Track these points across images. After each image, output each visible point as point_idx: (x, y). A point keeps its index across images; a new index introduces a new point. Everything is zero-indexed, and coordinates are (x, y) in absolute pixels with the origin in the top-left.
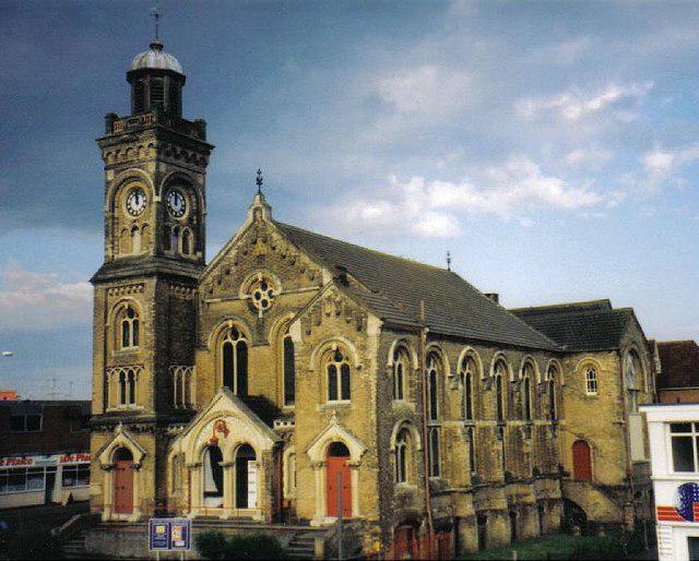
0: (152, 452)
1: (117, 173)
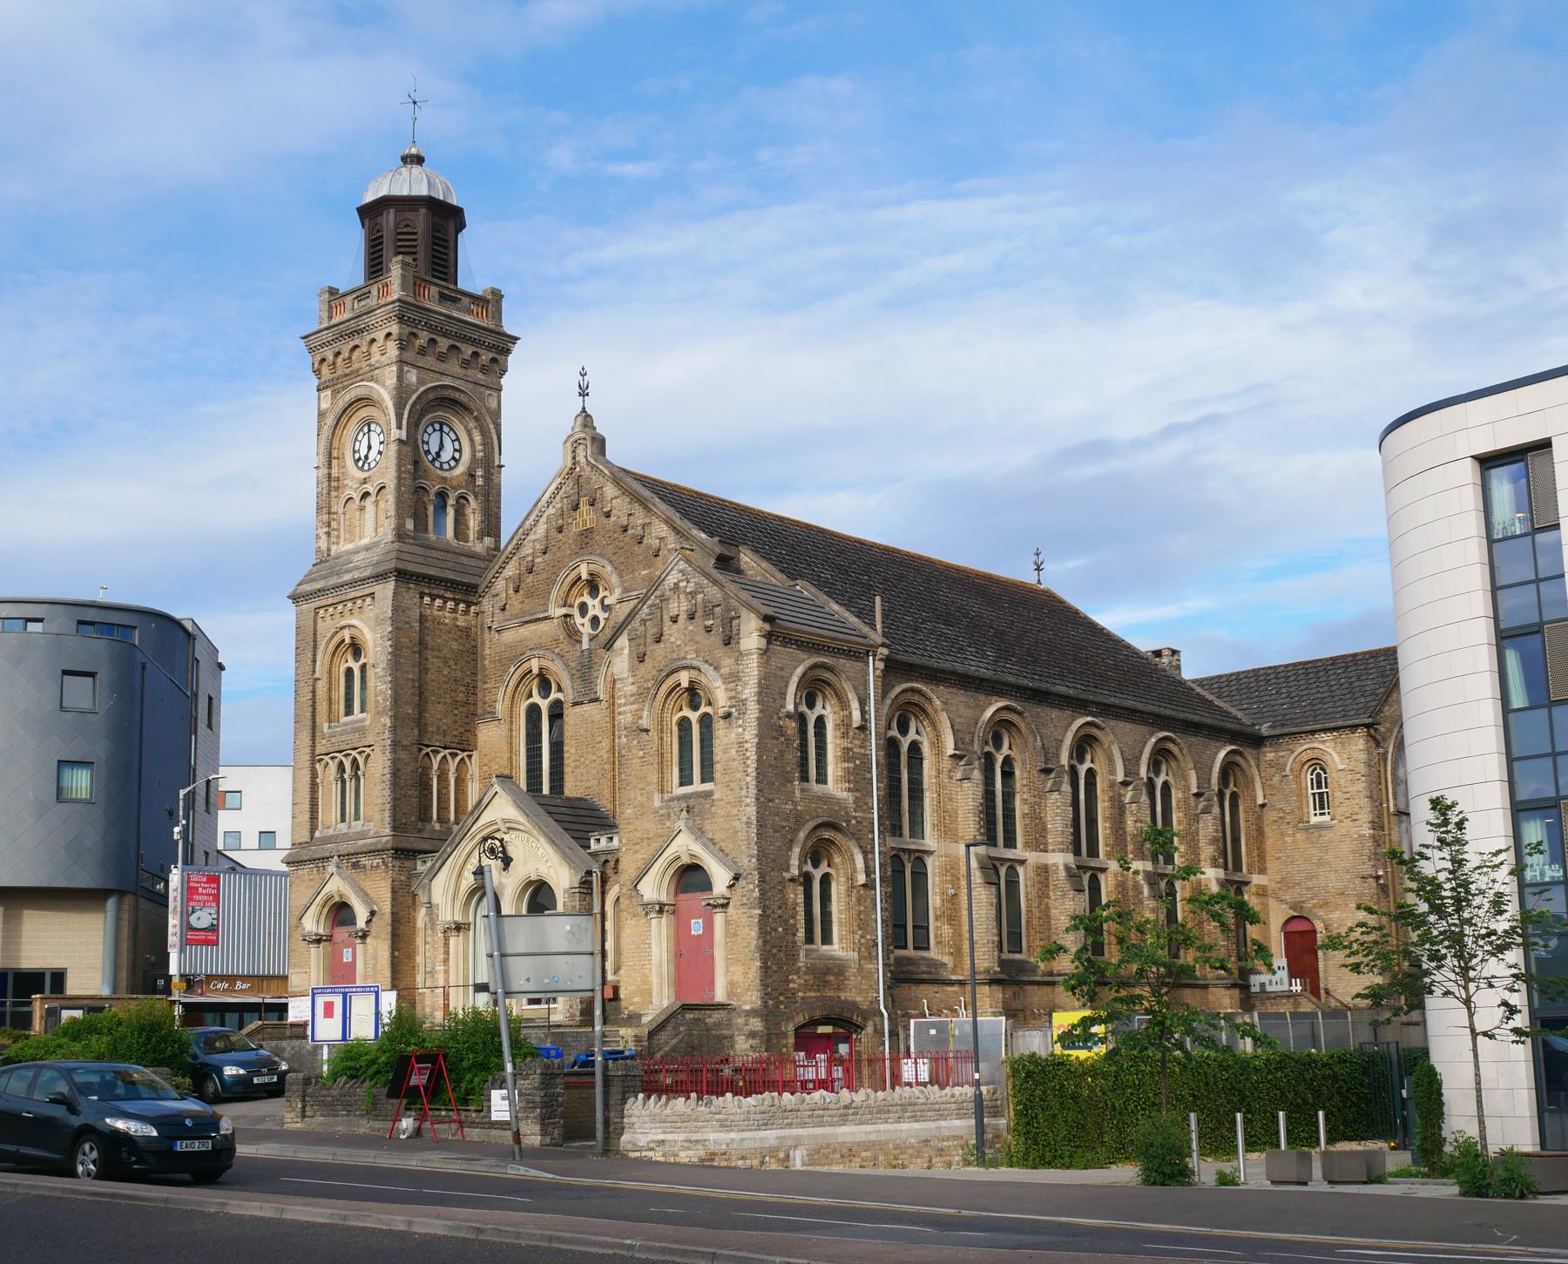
0: (386, 907)
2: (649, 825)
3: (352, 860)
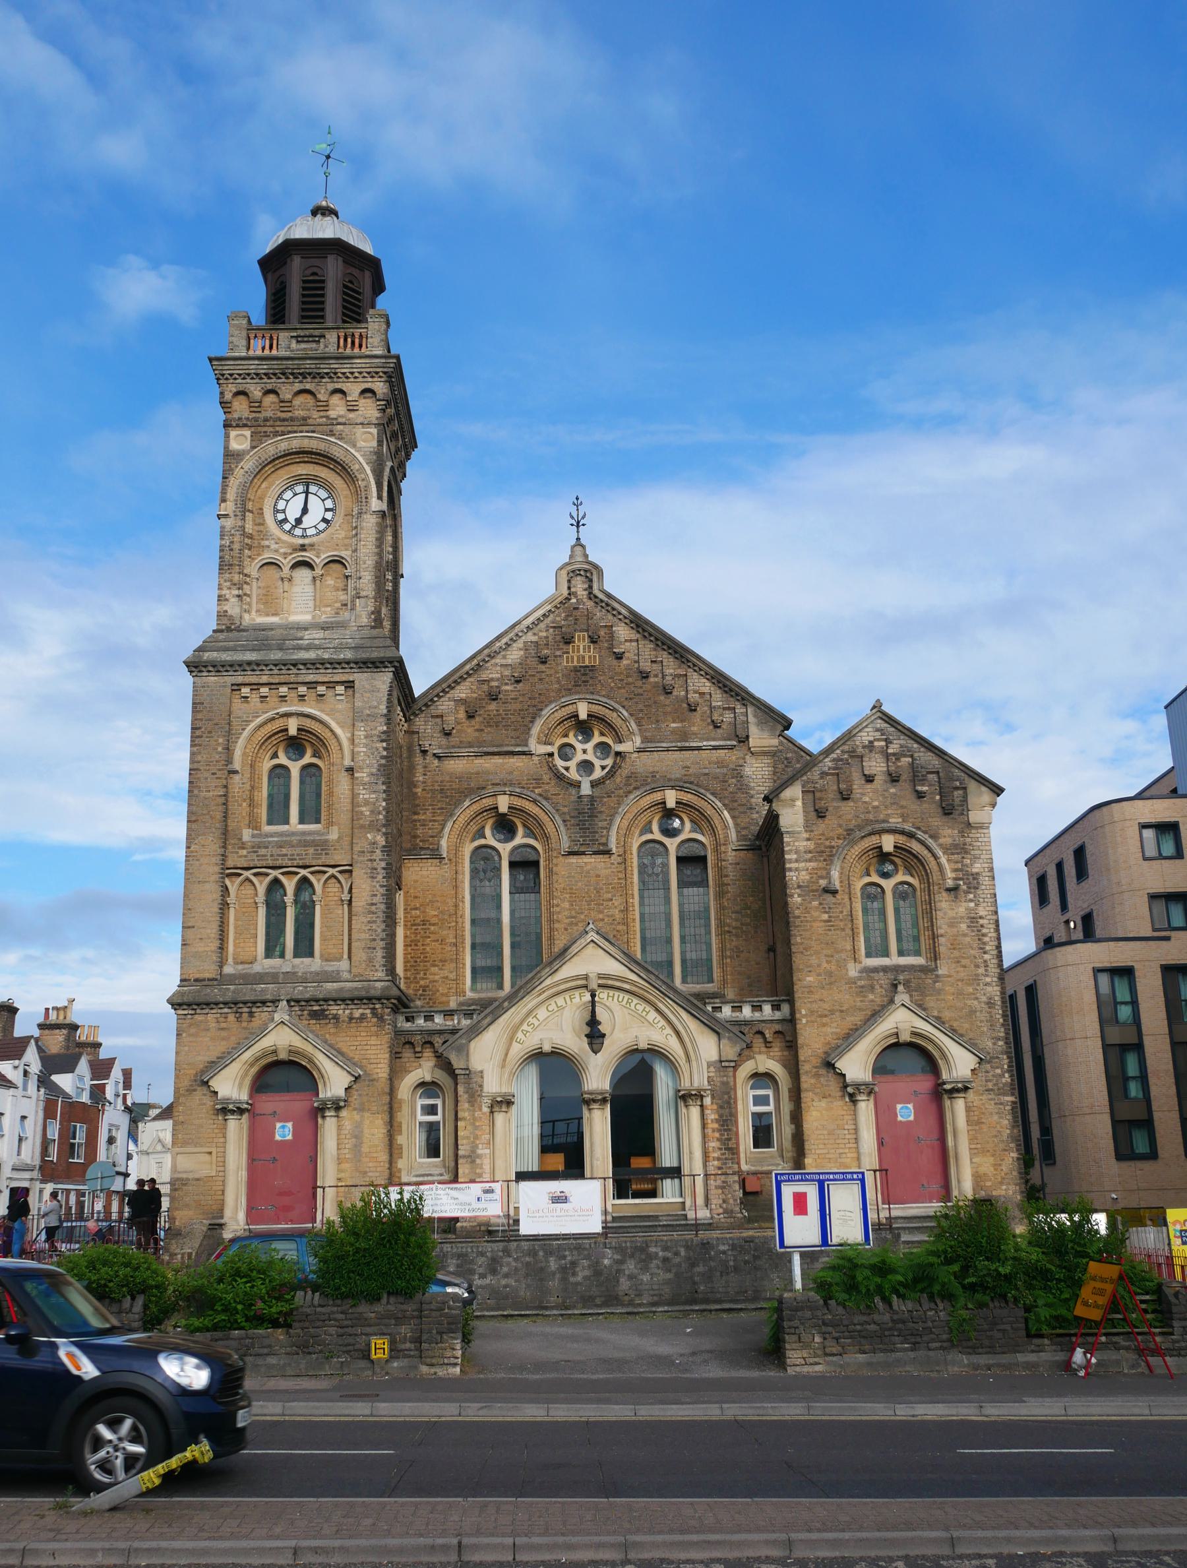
2: (846, 998)
3: (314, 1009)
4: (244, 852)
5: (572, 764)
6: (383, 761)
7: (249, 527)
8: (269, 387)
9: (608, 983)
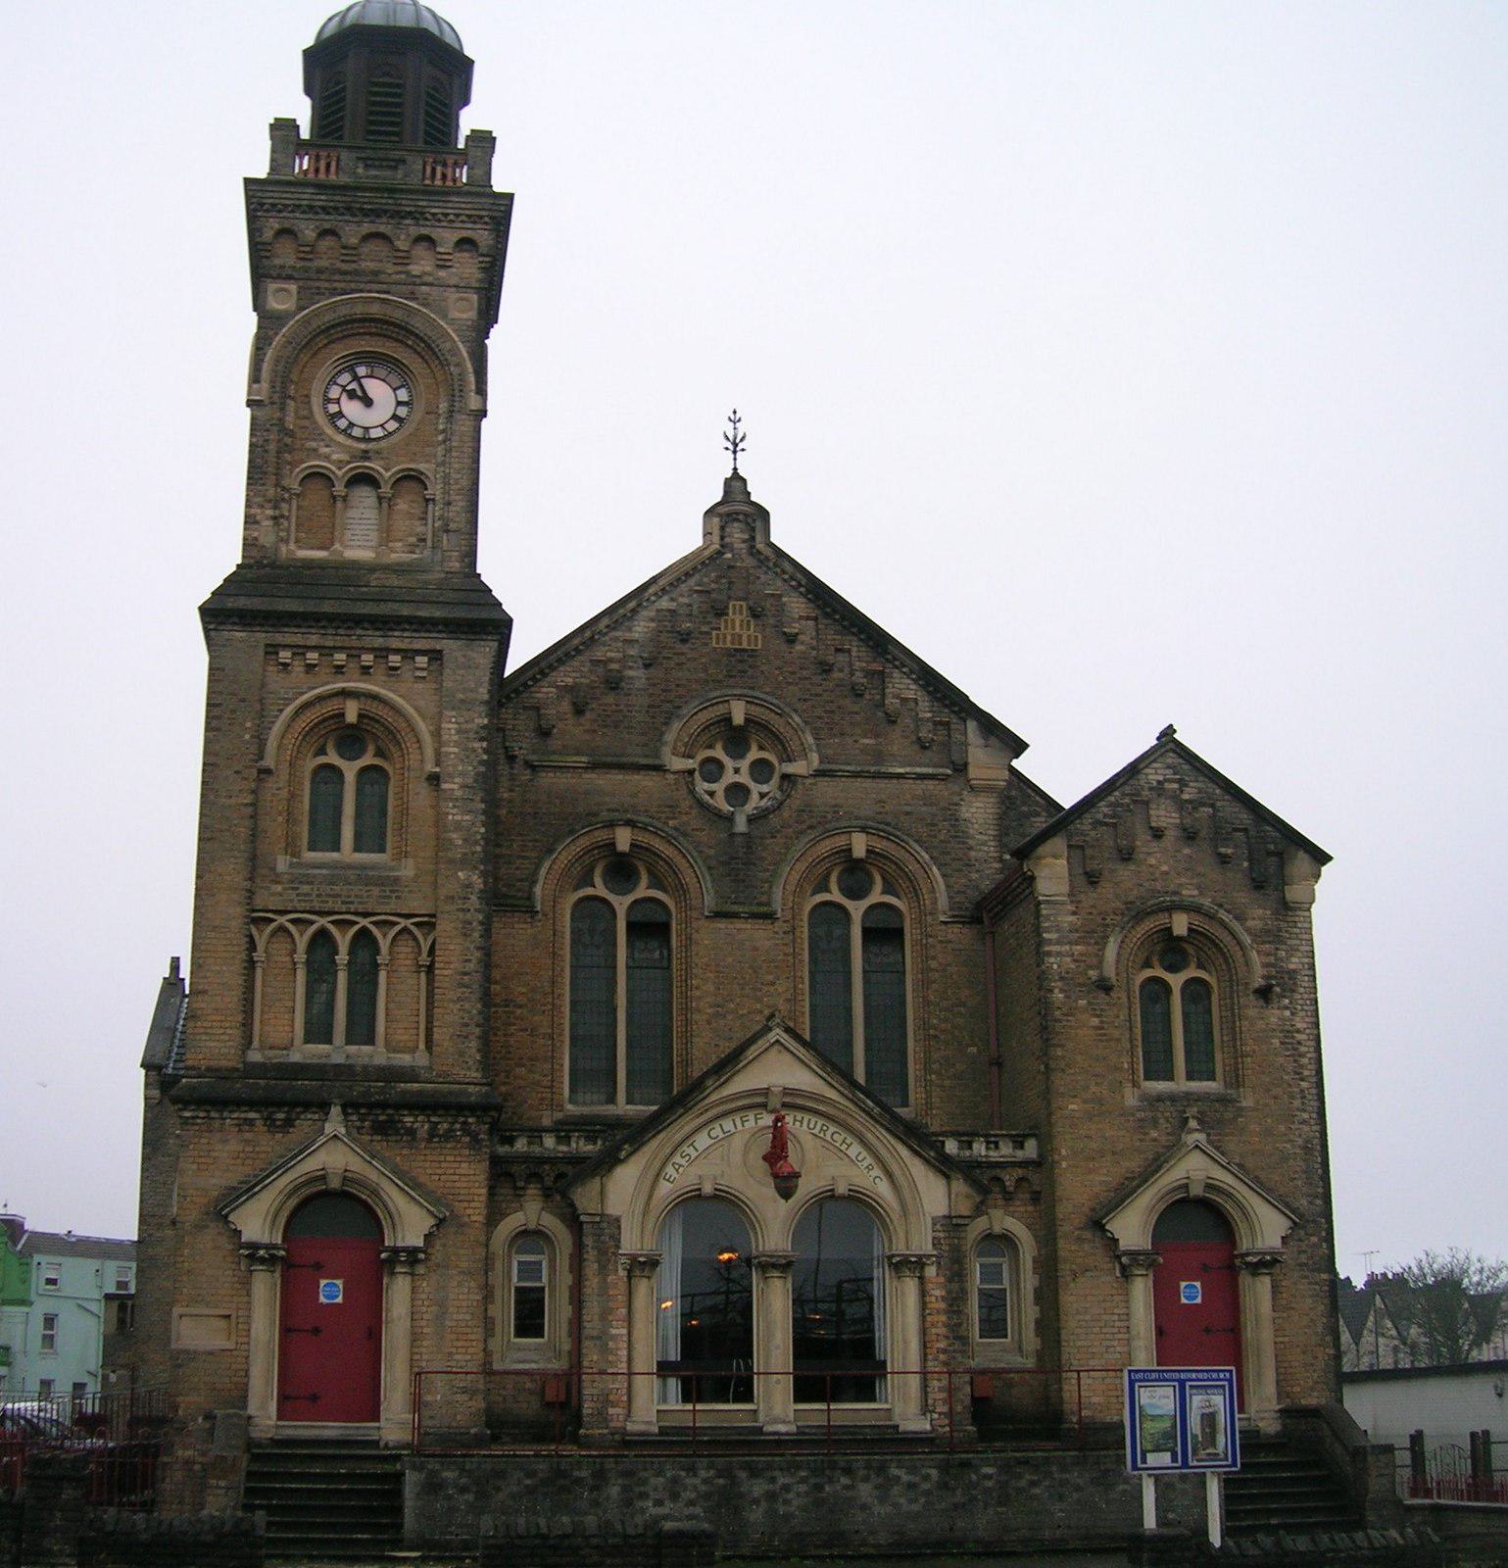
1: (305, 298)
4: (279, 888)
5: (718, 788)
6: (482, 769)
7: (290, 422)
8: (327, 226)
9: (795, 1101)
